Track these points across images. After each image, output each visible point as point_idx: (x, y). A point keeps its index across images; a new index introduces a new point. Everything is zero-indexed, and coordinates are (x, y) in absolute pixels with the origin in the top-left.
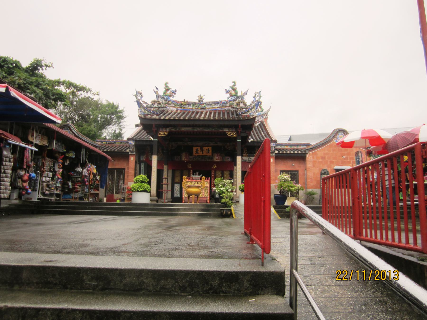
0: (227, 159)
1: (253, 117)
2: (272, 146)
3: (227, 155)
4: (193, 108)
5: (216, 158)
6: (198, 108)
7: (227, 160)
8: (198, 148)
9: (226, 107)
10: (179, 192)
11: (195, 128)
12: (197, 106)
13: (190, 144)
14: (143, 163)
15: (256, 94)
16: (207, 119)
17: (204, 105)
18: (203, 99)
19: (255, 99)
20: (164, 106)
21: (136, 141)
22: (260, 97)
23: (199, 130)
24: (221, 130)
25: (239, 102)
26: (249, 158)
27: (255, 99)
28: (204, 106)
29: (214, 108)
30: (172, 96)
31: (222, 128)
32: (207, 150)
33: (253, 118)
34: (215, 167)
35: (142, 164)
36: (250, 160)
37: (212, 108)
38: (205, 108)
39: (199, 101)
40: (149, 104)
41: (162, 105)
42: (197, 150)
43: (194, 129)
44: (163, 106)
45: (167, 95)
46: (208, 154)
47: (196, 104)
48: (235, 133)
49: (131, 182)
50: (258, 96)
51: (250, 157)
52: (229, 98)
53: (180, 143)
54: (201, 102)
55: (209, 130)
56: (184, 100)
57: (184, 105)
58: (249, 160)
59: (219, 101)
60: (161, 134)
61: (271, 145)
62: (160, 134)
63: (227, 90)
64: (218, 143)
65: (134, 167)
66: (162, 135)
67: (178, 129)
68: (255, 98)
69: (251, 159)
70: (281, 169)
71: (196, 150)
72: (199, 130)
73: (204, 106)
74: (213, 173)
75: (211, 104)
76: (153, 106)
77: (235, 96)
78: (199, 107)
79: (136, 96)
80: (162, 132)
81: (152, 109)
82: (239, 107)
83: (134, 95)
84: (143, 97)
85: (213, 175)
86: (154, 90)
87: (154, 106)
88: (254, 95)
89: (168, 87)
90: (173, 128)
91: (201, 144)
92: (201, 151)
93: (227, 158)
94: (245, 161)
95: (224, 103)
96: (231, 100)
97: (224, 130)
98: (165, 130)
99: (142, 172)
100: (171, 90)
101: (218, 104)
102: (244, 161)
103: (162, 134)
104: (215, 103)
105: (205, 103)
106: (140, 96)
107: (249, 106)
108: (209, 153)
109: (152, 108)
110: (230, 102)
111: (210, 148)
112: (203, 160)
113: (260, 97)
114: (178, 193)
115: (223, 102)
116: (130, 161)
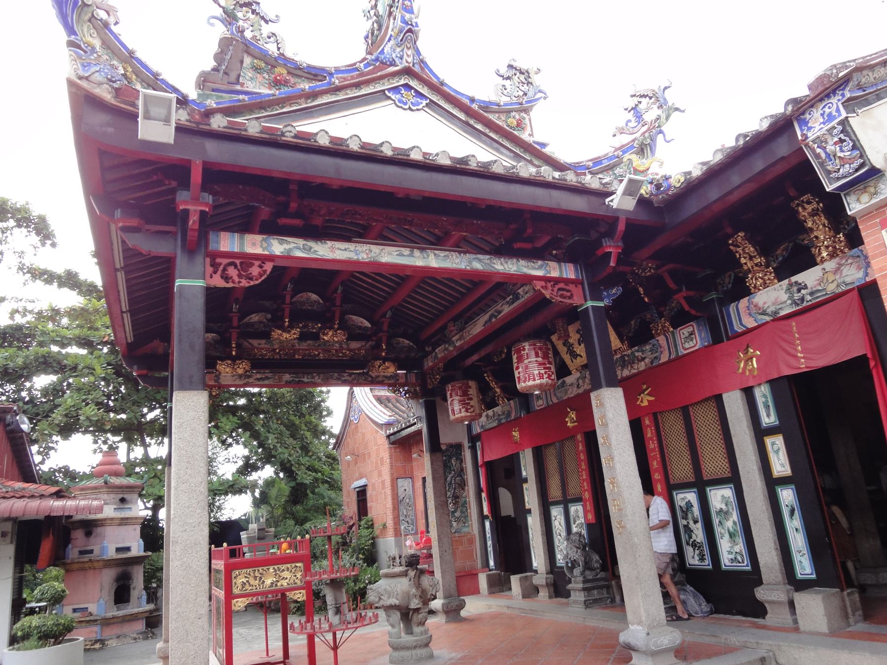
26: (791, 285)
36: (802, 299)
51: (794, 279)
58: (797, 296)
61: (811, 135)
69: (801, 287)
93: (685, 331)
94: (776, 313)
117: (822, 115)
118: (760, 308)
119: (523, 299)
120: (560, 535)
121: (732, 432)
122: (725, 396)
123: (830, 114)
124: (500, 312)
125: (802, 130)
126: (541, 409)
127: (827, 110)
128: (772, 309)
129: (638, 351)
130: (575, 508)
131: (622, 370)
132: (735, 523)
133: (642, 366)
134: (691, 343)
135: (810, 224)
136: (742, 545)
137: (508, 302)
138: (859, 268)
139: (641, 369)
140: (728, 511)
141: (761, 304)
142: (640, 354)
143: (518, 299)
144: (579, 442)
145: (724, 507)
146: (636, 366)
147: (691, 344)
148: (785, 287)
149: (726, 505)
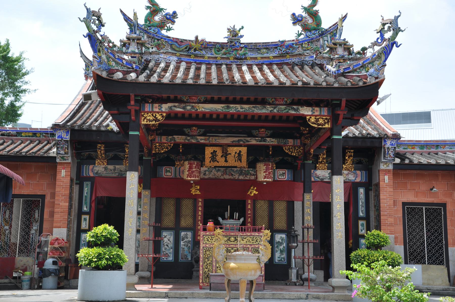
0: (281, 175)
1: (377, 80)
2: (388, 148)
3: (280, 165)
4: (216, 58)
5: (265, 174)
6: (228, 58)
7: (282, 178)
8: (215, 149)
9: (293, 56)
10: (172, 250)
11: (232, 105)
12: (225, 54)
13: (202, 141)
14: (89, 183)
15: (384, 25)
16: (265, 85)
17: (243, 50)
18: (242, 36)
19: (382, 36)
20: (154, 50)
21: (73, 131)
22: (397, 30)
23: (241, 110)
24: (293, 112)
25: (335, 44)
27: (382, 36)
28: (241, 52)
29: (265, 58)
30: (166, 28)
31: (295, 107)
32: (237, 155)
33: (377, 82)
34: (255, 192)
35: (85, 183)
37: (262, 58)
38: (246, 58)
39: (231, 42)
40: (115, 43)
41: (149, 48)
42: (214, 154)
43: (228, 107)
44: (151, 50)
45: (155, 24)
46: (237, 164)
47: (223, 48)
48: (326, 119)
49: (60, 227)
50: (389, 27)
52: (299, 35)
53: (179, 139)
54: (235, 43)
55: (264, 111)
56: (197, 38)
57: (195, 50)
59: (279, 41)
60: (148, 118)
61: (386, 146)
62: (145, 118)
63: (297, 15)
64: (268, 139)
65: (68, 192)
66: (150, 120)
67: (189, 108)
68: (383, 33)
70: (405, 200)
71: (211, 153)
72: (241, 110)
73: (241, 52)
74: (249, 207)
75: (259, 49)
76: (128, 48)
77: (315, 29)
78: (232, 55)
79: (87, 21)
80: (149, 114)
81: (126, 57)
82: (336, 56)
83: (82, 19)
84: (103, 26)
85: (249, 212)
86: (121, 11)
87: (130, 50)
88: (378, 26)
89: (157, 5)
90: (176, 104)
91: (228, 141)
92: (222, 157)
93: (281, 172)
94: (323, 179)
95: (290, 46)
96: (306, 41)
97: (301, 113)
98: (157, 110)
99: (86, 204)
100: (164, 14)
101: (276, 48)
102: (319, 180)
103: (151, 118)
104: (267, 46)
105: (245, 47)
106: (97, 22)
107: (359, 53)
108: (241, 162)
109: (125, 53)
110: (304, 45)
111: (244, 150)
112: (227, 177)
113: (397, 30)
114: (170, 253)
115: (286, 44)
116: (58, 177)
117: (391, 142)
118: (317, 176)
119: (269, 143)
120: (167, 246)
121: (295, 215)
122: (295, 202)
123: (392, 144)
124: (248, 142)
125: (384, 143)
126: (165, 178)
127: (392, 142)
128: (322, 177)
129: (252, 171)
130: (186, 233)
131: (240, 175)
132: (284, 247)
133: (253, 178)
134: (282, 177)
135: (347, 158)
136: (285, 255)
137: (256, 140)
138: (354, 177)
139: (251, 179)
140: (282, 242)
141: (318, 174)
142: (253, 172)
143: (264, 141)
144: (199, 201)
145: (280, 241)
146: (249, 177)
147: (283, 177)
148: (328, 172)
149: (282, 240)
